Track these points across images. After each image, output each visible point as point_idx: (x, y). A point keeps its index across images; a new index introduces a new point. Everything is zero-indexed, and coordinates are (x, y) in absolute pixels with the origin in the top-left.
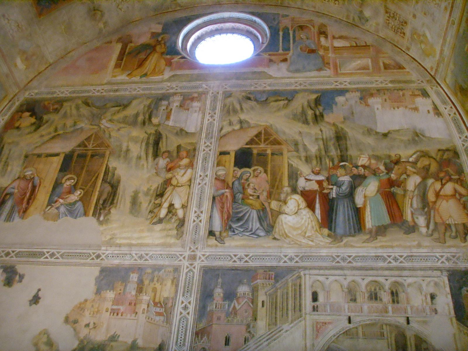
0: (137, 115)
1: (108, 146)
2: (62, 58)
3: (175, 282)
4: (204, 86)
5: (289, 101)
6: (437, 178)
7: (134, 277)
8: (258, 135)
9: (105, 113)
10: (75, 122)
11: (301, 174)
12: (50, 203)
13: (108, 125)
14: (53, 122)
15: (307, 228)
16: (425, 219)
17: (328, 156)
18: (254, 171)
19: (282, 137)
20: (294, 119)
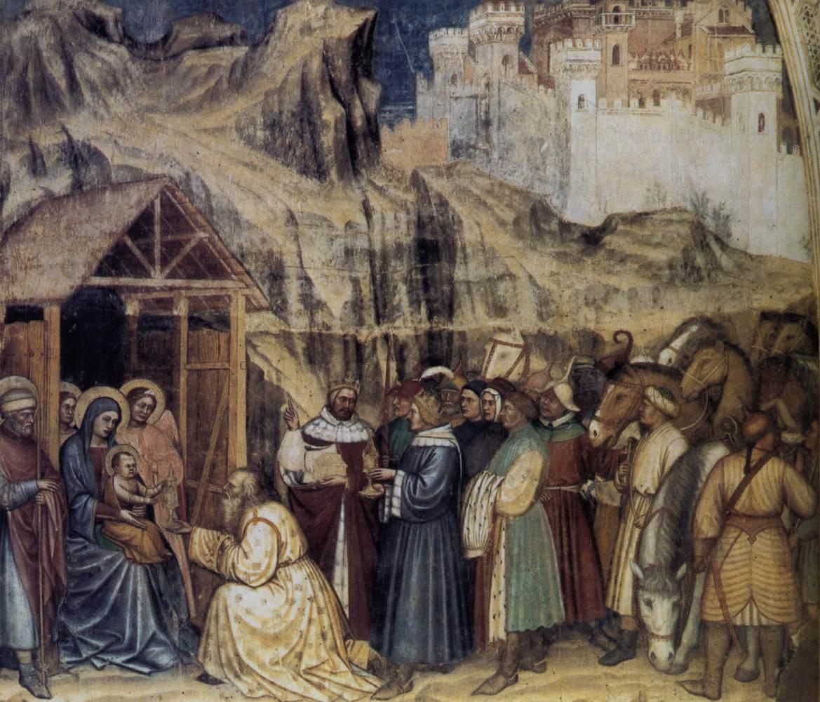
5: (254, 46)
6: (740, 444)
8: (140, 227)
11: (292, 413)
15: (303, 636)
16: (675, 606)
18: (133, 396)
20: (269, 148)
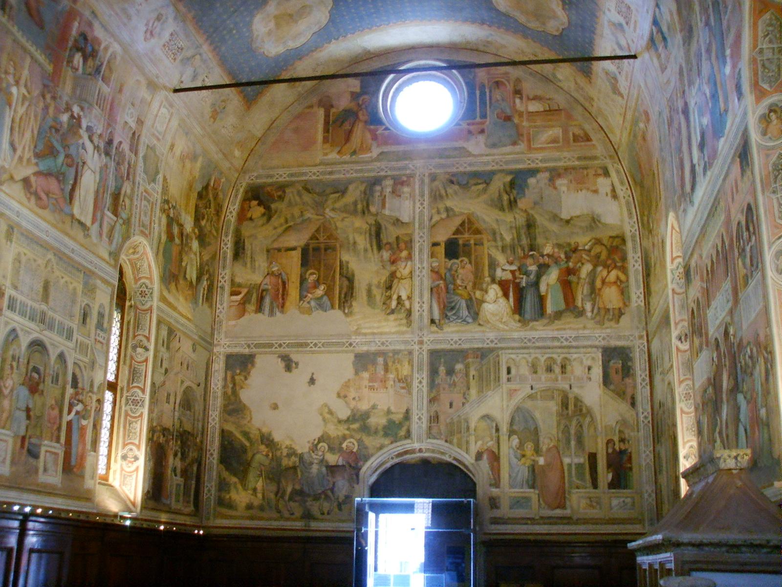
0: (355, 203)
1: (336, 239)
2: (269, 129)
3: (410, 362)
4: (410, 166)
6: (606, 266)
7: (380, 360)
8: (462, 224)
9: (326, 200)
10: (302, 212)
11: (498, 265)
12: (302, 297)
13: (332, 214)
14: (281, 212)
15: (503, 315)
17: (520, 246)
18: (462, 261)
19: (482, 226)
20: (491, 206)
